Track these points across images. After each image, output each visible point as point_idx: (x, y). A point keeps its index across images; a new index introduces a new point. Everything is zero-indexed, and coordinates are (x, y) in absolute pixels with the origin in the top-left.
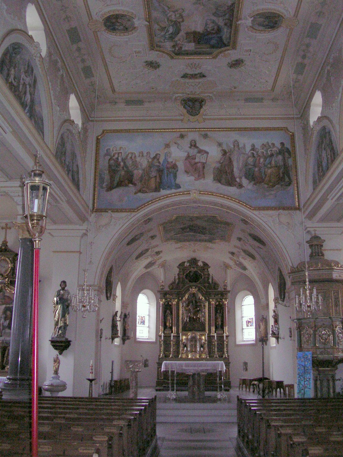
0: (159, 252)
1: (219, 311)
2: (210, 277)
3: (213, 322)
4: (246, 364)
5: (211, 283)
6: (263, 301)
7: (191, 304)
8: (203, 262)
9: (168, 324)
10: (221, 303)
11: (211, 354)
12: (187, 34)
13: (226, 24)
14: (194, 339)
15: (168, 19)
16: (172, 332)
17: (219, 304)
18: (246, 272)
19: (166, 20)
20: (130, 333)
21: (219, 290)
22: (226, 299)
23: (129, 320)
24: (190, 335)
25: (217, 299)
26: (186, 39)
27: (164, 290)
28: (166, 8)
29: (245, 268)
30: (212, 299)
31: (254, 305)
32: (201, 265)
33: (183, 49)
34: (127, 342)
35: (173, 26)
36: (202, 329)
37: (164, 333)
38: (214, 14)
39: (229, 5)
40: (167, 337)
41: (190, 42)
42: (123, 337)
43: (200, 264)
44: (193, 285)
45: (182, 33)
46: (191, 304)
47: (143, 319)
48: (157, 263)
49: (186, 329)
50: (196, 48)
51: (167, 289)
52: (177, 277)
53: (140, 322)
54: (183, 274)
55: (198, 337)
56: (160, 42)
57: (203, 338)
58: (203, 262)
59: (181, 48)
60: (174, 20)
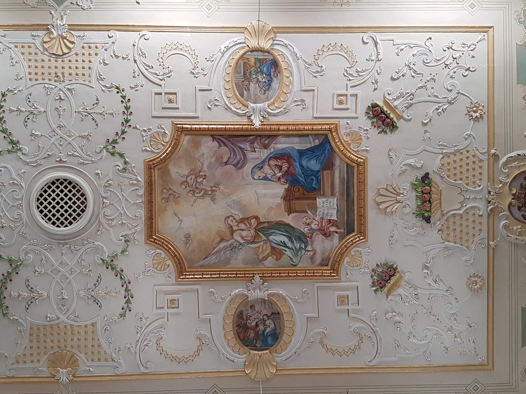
12: (290, 210)
13: (266, 147)
15: (253, 242)
19: (254, 246)
26: (306, 212)
28: (222, 245)
33: (335, 218)
35: (267, 236)
38: (239, 165)
39: (216, 143)
41: (314, 208)
45: (289, 219)
50: (333, 194)
56: (312, 258)
59: (330, 221)
60: (253, 231)
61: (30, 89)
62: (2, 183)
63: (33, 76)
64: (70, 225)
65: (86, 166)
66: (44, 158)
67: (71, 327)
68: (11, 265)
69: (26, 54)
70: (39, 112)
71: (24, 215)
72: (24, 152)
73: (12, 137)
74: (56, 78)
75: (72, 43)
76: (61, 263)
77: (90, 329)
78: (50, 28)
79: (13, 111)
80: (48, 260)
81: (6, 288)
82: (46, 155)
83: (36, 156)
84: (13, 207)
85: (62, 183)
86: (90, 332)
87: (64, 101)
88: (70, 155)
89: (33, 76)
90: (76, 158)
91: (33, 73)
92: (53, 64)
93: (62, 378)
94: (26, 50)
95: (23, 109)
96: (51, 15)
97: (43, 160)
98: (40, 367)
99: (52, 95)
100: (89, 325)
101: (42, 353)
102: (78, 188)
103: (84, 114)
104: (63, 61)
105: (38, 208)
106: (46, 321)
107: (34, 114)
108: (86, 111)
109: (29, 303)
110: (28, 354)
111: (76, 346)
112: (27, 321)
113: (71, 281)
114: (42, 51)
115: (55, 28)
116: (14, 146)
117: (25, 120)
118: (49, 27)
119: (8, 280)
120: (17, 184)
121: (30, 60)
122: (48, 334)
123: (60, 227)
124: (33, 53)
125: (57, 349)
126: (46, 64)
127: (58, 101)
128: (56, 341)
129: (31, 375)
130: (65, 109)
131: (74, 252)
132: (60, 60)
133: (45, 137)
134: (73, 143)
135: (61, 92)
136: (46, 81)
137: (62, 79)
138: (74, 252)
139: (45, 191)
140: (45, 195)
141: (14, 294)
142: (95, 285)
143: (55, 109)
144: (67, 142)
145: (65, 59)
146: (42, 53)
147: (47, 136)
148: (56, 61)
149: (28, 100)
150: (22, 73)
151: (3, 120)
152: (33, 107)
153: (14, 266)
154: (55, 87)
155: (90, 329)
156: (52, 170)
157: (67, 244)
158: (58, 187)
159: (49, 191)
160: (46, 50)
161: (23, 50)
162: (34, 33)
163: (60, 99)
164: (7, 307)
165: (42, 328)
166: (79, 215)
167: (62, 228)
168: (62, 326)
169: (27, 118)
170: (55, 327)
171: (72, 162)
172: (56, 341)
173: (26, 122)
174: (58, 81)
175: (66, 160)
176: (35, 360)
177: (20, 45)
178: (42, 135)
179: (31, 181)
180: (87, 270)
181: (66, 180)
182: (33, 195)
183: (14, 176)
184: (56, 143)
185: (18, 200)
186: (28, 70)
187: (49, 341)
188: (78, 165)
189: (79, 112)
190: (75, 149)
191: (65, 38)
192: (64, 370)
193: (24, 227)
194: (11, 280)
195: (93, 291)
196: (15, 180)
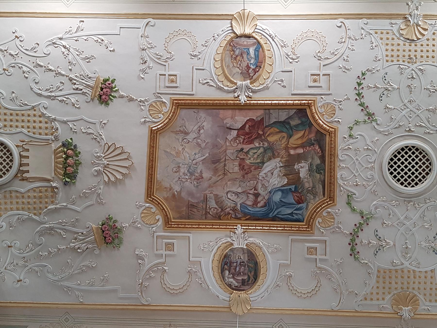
61: (386, 69)
62: (358, 148)
63: (389, 58)
64: (416, 185)
65: (431, 135)
66: (395, 128)
67: (414, 272)
68: (363, 217)
69: (384, 39)
70: (394, 89)
71: (376, 176)
72: (378, 122)
73: (368, 110)
74: (409, 60)
75: (425, 30)
76: (406, 217)
77: (429, 275)
78: (408, 17)
79: (371, 88)
80: (395, 214)
81: (358, 237)
82: (397, 126)
83: (389, 126)
84: (367, 169)
85: (410, 150)
86: (429, 277)
87: (415, 79)
88: (418, 126)
89: (389, 58)
90: (423, 128)
91: (390, 55)
92: (407, 47)
93: (405, 314)
94: (384, 36)
95: (380, 86)
96: (408, 6)
97: (393, 129)
98: (384, 304)
99: (405, 74)
100: (429, 271)
101: (386, 293)
102: (424, 153)
103: (432, 90)
104: (416, 45)
105: (389, 170)
106: (392, 265)
107: (389, 90)
108: (434, 88)
109: (377, 250)
110: (374, 293)
111: (416, 288)
112: (375, 264)
113: (414, 233)
114: (398, 36)
115: (413, 17)
116: (370, 117)
117: (380, 95)
118: (407, 16)
119: (359, 229)
120: (371, 150)
121: (387, 44)
122: (393, 277)
123: (407, 187)
124: (390, 39)
125: (400, 290)
126: (401, 48)
127: (410, 80)
128: (399, 283)
129: (376, 311)
130: (415, 87)
131: (418, 209)
132: (413, 44)
133: (396, 110)
134: (421, 115)
135: (413, 72)
136: (401, 62)
137: (415, 61)
138: (418, 209)
139: (395, 156)
140: (395, 160)
141: (365, 241)
142: (434, 237)
143: (407, 86)
144: (416, 114)
145: (417, 43)
146: (399, 39)
147: (399, 109)
148: (410, 45)
149: (385, 78)
150: (380, 55)
151: (362, 95)
152: (389, 85)
153: (365, 218)
154: (408, 68)
155: (429, 275)
156: (401, 139)
157: (411, 201)
158: (406, 153)
159: (399, 156)
160: (402, 35)
161: (382, 36)
162: (393, 21)
163: (413, 77)
164: (359, 252)
165: (388, 272)
166: (424, 177)
167: (409, 188)
168: (406, 271)
169: (382, 93)
170: (400, 272)
171: (419, 132)
172: (399, 283)
173: (381, 97)
174: (411, 63)
175: (414, 130)
176: (381, 298)
177: (385, 32)
178: (394, 108)
179: (383, 148)
180: (429, 225)
181: (413, 147)
182: (386, 159)
183: (369, 143)
184: (406, 115)
185: (371, 163)
186: (385, 53)
187: (393, 283)
188: (424, 134)
189: (427, 89)
190: (422, 121)
191: (420, 26)
192: (406, 308)
193: (375, 186)
194: (362, 230)
195: (432, 242)
196: (369, 146)
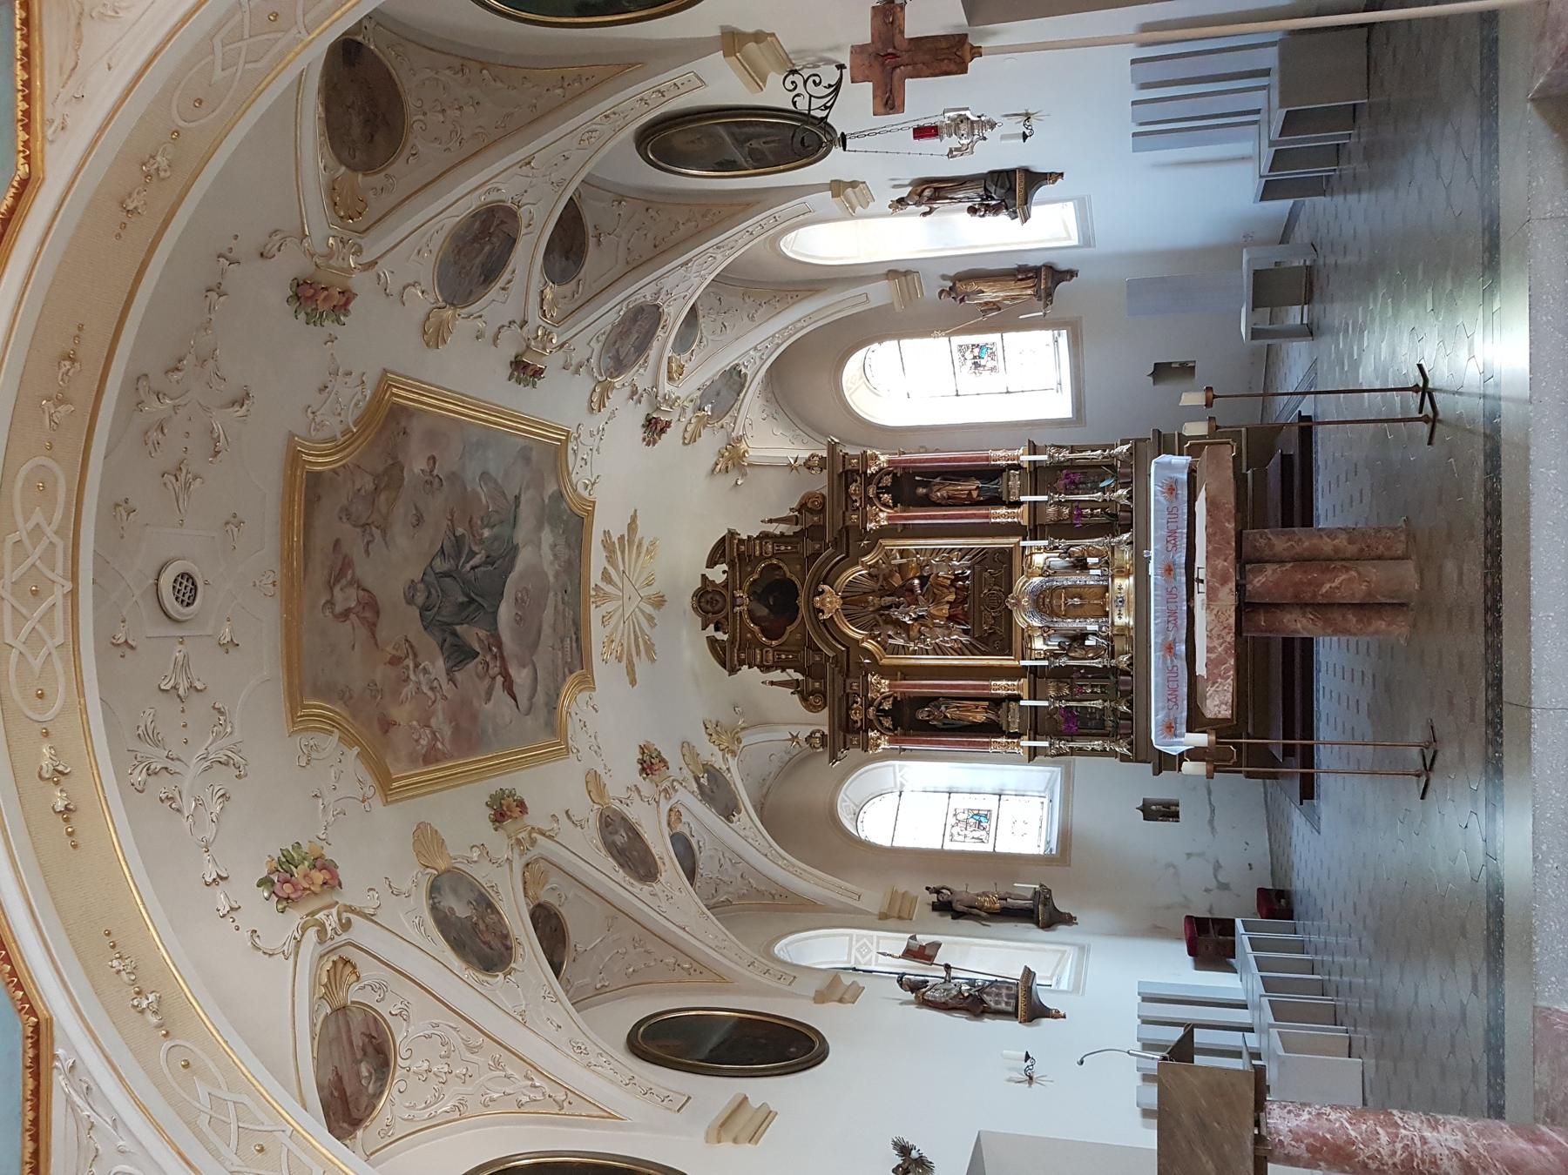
0: (642, 762)
1: (921, 491)
2: (777, 529)
3: (972, 516)
4: (1161, 371)
5: (798, 528)
6: (880, 294)
7: (895, 613)
8: (711, 563)
9: (980, 717)
10: (887, 481)
11: (1117, 521)
14: (1044, 602)
16: (1018, 698)
17: (887, 490)
18: (749, 373)
20: (1025, 888)
21: (825, 492)
22: (865, 459)
23: (965, 888)
24: (1026, 620)
25: (869, 501)
27: (827, 732)
29: (735, 379)
30: (865, 520)
31: (905, 343)
32: (724, 572)
34: (1062, 905)
36: (1001, 566)
37: (1018, 735)
40: (1037, 724)
42: (1037, 924)
43: (718, 574)
44: (809, 601)
46: (895, 613)
47: (965, 816)
48: (718, 763)
49: (999, 636)
51: (821, 721)
52: (777, 675)
53: (977, 834)
54: (763, 645)
55: (1036, 580)
57: (1039, 559)
58: (711, 563)
